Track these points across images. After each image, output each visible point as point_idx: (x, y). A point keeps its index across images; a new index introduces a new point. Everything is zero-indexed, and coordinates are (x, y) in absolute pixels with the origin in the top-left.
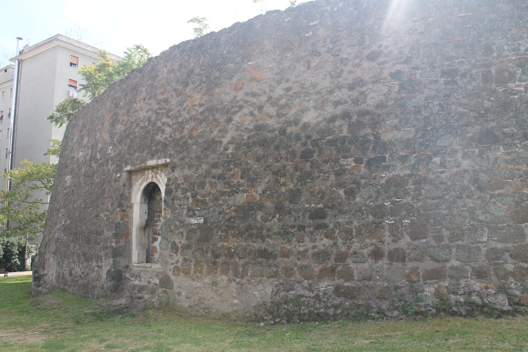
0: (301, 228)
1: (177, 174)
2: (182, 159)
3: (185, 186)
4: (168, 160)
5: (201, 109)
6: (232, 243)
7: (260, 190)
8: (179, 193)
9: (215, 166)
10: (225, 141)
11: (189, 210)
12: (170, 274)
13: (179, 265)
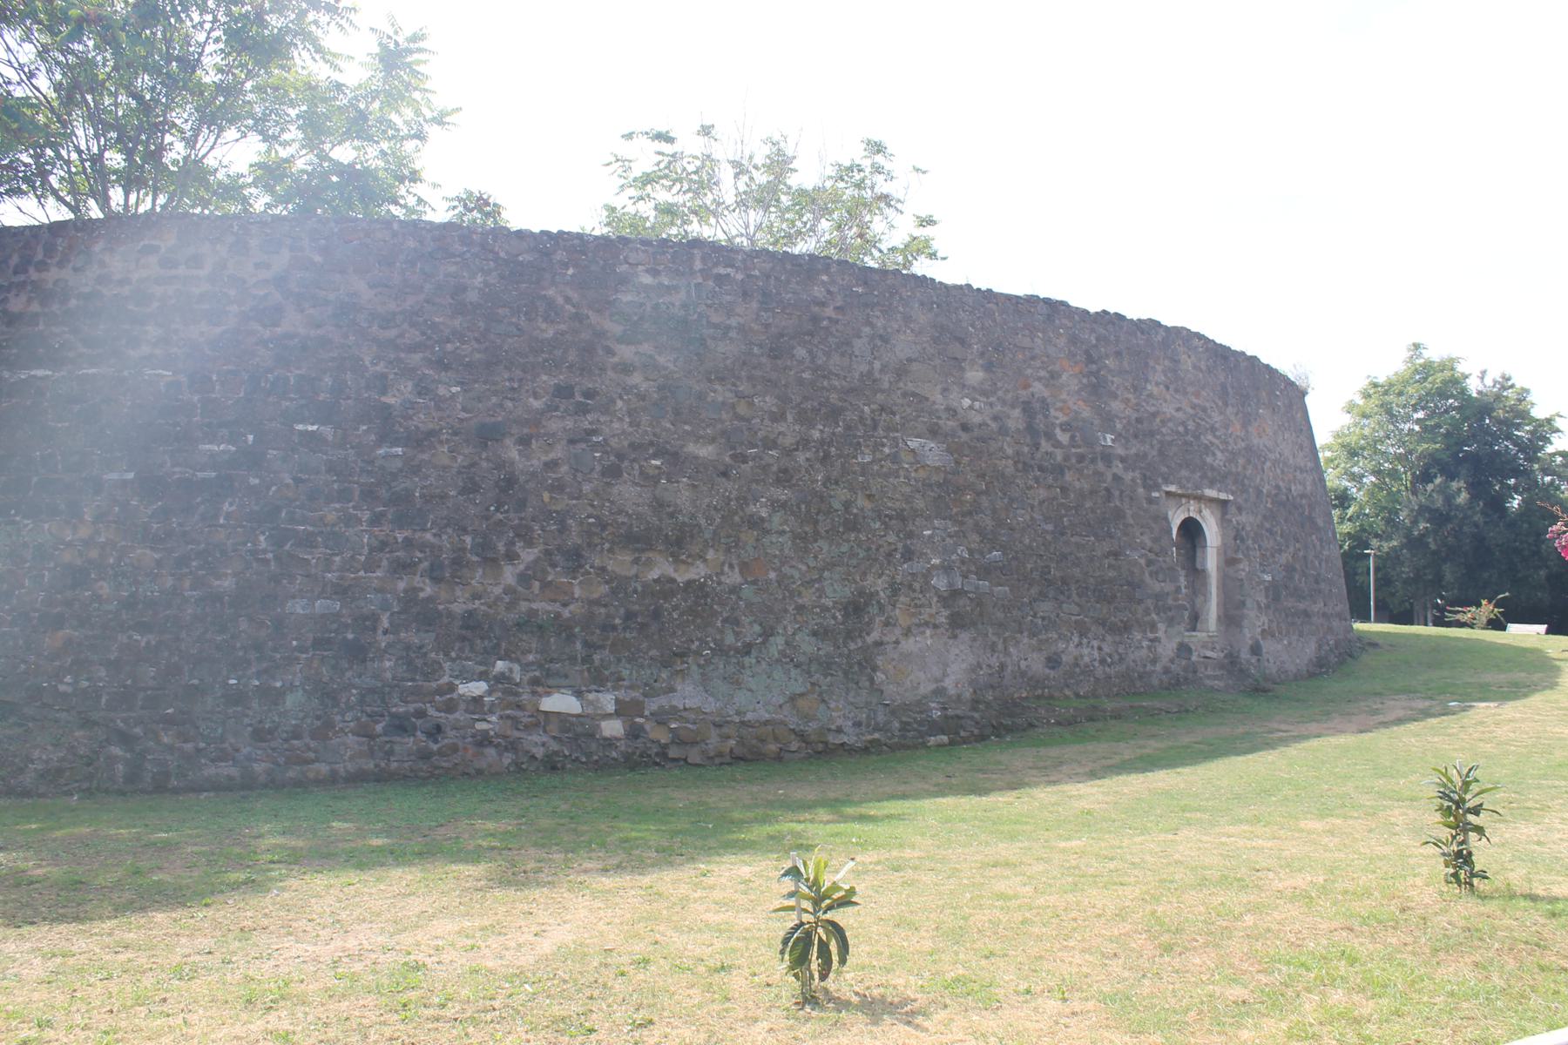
1: (1243, 518)
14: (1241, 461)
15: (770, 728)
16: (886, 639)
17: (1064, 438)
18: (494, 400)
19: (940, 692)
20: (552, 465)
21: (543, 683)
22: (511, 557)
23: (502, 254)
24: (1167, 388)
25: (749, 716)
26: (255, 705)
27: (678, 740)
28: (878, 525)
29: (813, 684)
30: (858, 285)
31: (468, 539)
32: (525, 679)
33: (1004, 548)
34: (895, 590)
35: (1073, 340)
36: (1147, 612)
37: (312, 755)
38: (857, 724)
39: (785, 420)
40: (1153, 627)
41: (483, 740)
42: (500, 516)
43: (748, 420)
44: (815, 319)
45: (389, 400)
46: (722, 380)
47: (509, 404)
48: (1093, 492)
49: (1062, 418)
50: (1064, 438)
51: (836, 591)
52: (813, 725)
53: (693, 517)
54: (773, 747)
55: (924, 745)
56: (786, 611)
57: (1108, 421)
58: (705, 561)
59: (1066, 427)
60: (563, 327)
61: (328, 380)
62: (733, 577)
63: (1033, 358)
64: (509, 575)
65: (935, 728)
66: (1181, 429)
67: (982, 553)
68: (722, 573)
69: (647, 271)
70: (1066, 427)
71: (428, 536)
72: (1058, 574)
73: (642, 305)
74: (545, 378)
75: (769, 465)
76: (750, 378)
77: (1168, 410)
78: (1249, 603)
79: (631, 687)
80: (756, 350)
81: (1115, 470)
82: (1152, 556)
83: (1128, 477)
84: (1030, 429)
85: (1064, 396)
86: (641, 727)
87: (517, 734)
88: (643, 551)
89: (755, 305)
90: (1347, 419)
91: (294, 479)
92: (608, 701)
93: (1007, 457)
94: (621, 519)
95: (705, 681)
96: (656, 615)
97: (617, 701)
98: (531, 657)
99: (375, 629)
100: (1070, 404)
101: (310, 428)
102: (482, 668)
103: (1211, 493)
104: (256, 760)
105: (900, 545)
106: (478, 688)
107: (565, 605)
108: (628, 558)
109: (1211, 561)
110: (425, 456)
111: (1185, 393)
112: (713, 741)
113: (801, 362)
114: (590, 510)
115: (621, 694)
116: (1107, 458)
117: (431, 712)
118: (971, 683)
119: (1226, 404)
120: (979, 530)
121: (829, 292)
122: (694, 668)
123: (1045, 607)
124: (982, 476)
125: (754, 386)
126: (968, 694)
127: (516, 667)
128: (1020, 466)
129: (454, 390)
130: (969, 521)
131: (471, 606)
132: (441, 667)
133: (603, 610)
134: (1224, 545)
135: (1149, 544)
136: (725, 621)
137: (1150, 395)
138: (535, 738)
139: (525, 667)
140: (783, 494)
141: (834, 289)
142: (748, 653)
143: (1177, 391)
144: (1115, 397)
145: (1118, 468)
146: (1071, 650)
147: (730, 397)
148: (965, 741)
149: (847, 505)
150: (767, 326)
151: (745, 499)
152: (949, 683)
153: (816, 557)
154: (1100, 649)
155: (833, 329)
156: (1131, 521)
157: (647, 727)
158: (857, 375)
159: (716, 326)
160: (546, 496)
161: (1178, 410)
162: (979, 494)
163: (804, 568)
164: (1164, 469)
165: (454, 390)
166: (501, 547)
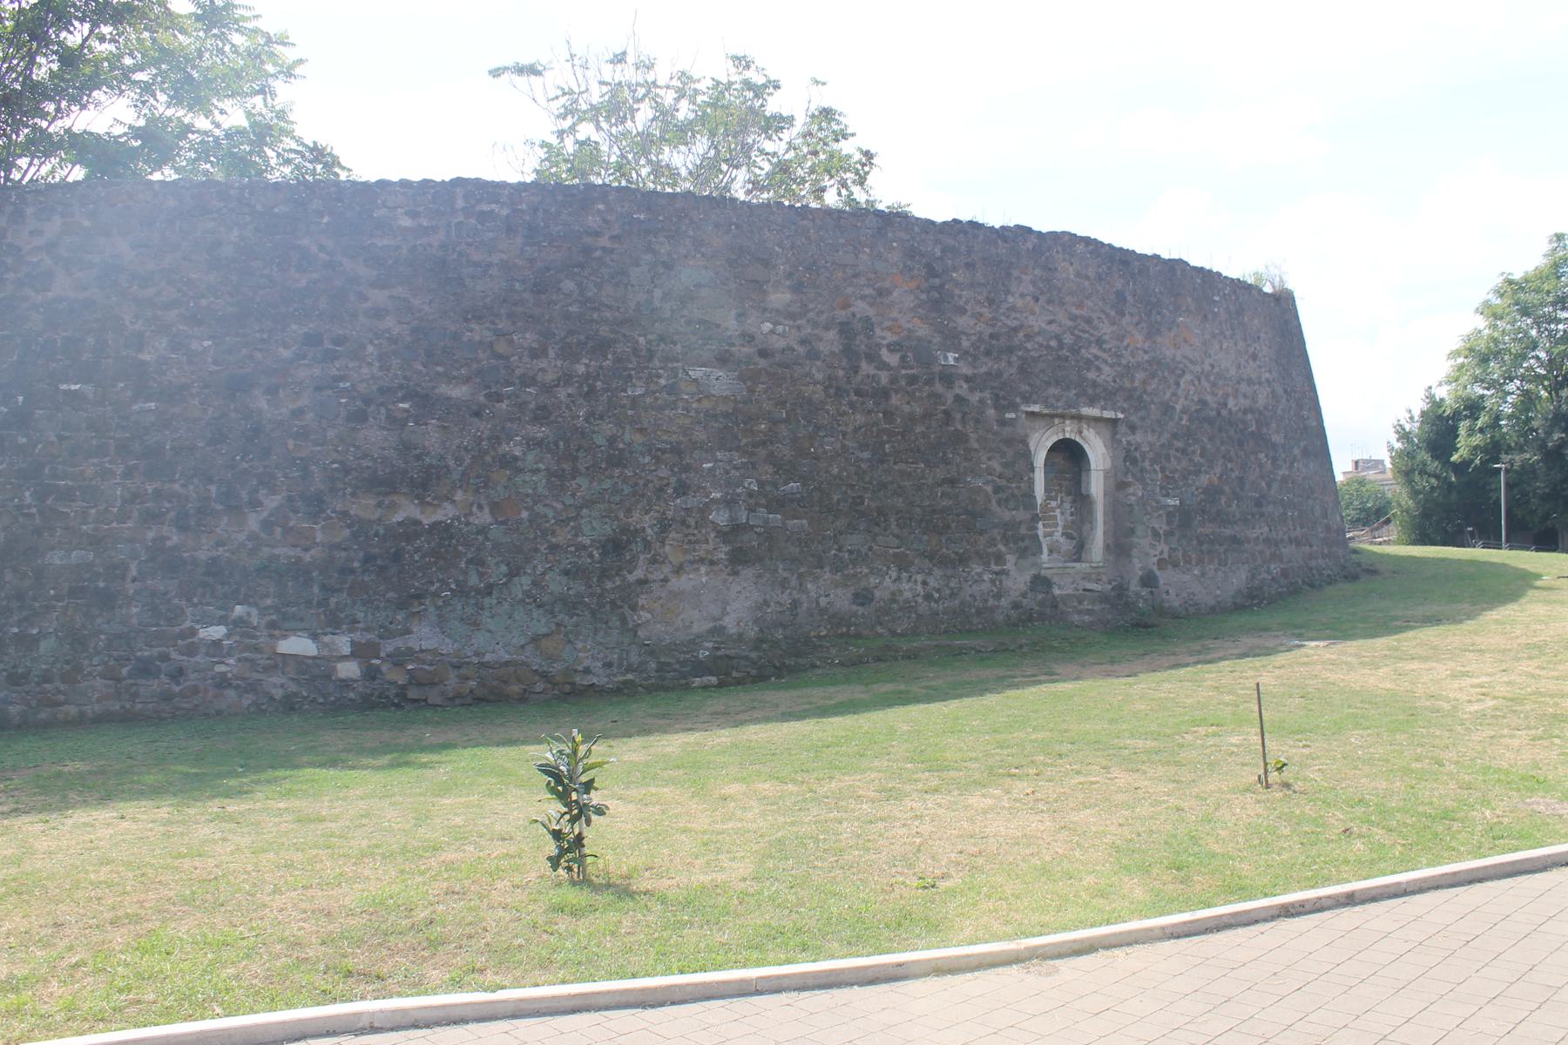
0: (1253, 515)
1: (1138, 437)
2: (1143, 419)
3: (1151, 455)
4: (1121, 416)
5: (1146, 357)
6: (1208, 529)
8: (1147, 464)
10: (1178, 407)
11: (1162, 488)
12: (1155, 568)
13: (1166, 556)
14: (1140, 376)
15: (512, 669)
16: (651, 577)
17: (892, 359)
18: (244, 351)
19: (718, 631)
20: (299, 413)
21: (278, 628)
22: (255, 504)
23: (259, 207)
24: (1037, 300)
25: (488, 657)
26: (11, 651)
27: (415, 680)
28: (647, 459)
29: (558, 625)
30: (639, 212)
31: (213, 489)
32: (263, 622)
33: (804, 480)
34: (664, 526)
35: (911, 254)
36: (992, 542)
37: (62, 698)
38: (608, 665)
39: (546, 356)
40: (1000, 559)
41: (223, 682)
42: (245, 465)
43: (507, 358)
44: (587, 250)
45: (146, 357)
46: (479, 319)
47: (258, 355)
48: (927, 415)
49: (890, 338)
50: (892, 359)
51: (595, 528)
52: (558, 666)
53: (442, 458)
54: (516, 689)
55: (687, 688)
56: (536, 550)
57: (951, 338)
58: (453, 502)
59: (892, 348)
60: (315, 276)
61: (91, 340)
62: (484, 517)
63: (856, 276)
64: (253, 522)
65: (701, 668)
67: (775, 485)
68: (471, 514)
69: (406, 214)
70: (892, 348)
71: (176, 487)
72: (873, 505)
73: (399, 247)
74: (294, 327)
75: (525, 403)
76: (510, 315)
77: (1037, 323)
78: (1140, 530)
79: (366, 629)
80: (517, 286)
81: (957, 391)
82: (1003, 482)
83: (974, 398)
84: (848, 352)
85: (895, 314)
86: (377, 669)
87: (255, 676)
88: (386, 494)
89: (519, 240)
90: (1481, 323)
91: (60, 438)
92: (343, 644)
93: (816, 383)
94: (365, 463)
95: (442, 622)
96: (397, 557)
97: (353, 643)
98: (269, 602)
99: (123, 578)
100: (903, 322)
101: (73, 387)
102: (222, 613)
103: (1094, 412)
104: (11, 703)
105: (673, 480)
106: (217, 632)
107: (306, 550)
108: (372, 502)
109: (1096, 486)
110: (177, 410)
111: (1062, 304)
112: (452, 682)
113: (569, 296)
114: (335, 455)
115: (357, 636)
116: (948, 378)
117: (174, 655)
118: (756, 622)
119: (1122, 314)
120: (771, 459)
121: (605, 221)
122: (432, 609)
123: (854, 541)
124: (782, 403)
125: (514, 323)
126: (752, 632)
127: (254, 611)
128: (832, 391)
129: (206, 343)
130: (762, 452)
131: (215, 553)
132: (183, 612)
133: (343, 554)
134: (1114, 467)
135: (999, 469)
136: (469, 562)
137: (1013, 308)
138: (274, 680)
139: (263, 611)
140: (540, 432)
141: (612, 218)
142: (490, 594)
143: (1049, 302)
144: (963, 311)
145: (962, 388)
146: (886, 585)
147: (488, 335)
148: (739, 682)
149: (612, 441)
150: (532, 261)
151: (498, 438)
152: (729, 622)
153: (573, 495)
154: (924, 583)
155: (607, 259)
156: (976, 446)
157: (384, 668)
158: (633, 305)
159: (477, 264)
160: (291, 444)
161: (1050, 322)
162: (775, 423)
163: (559, 506)
164: (1025, 388)
165: (206, 343)
166: (244, 495)
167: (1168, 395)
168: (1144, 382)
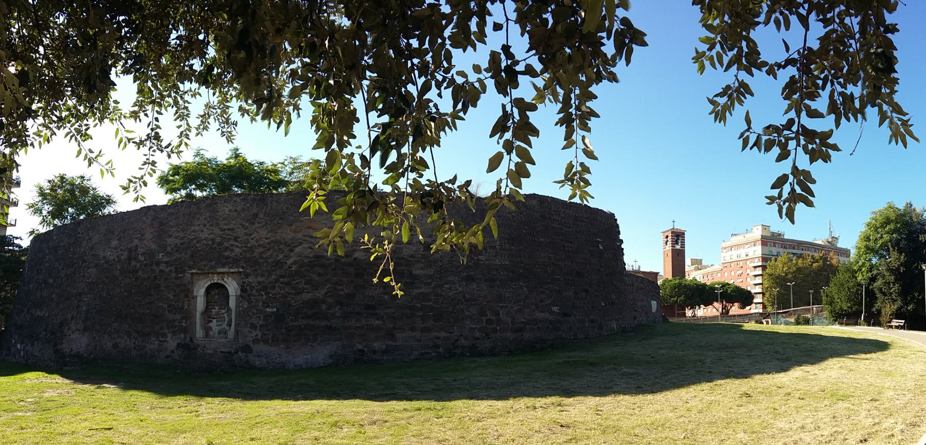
1: (251, 279)
7: (323, 292)
9: (281, 276)
10: (289, 262)
11: (264, 303)
12: (251, 344)
13: (259, 337)
14: (258, 251)
49: (143, 251)
50: (141, 258)
57: (163, 248)
66: (210, 243)
83: (167, 270)
109: (232, 303)
116: (158, 263)
167: (281, 257)
168: (262, 253)
